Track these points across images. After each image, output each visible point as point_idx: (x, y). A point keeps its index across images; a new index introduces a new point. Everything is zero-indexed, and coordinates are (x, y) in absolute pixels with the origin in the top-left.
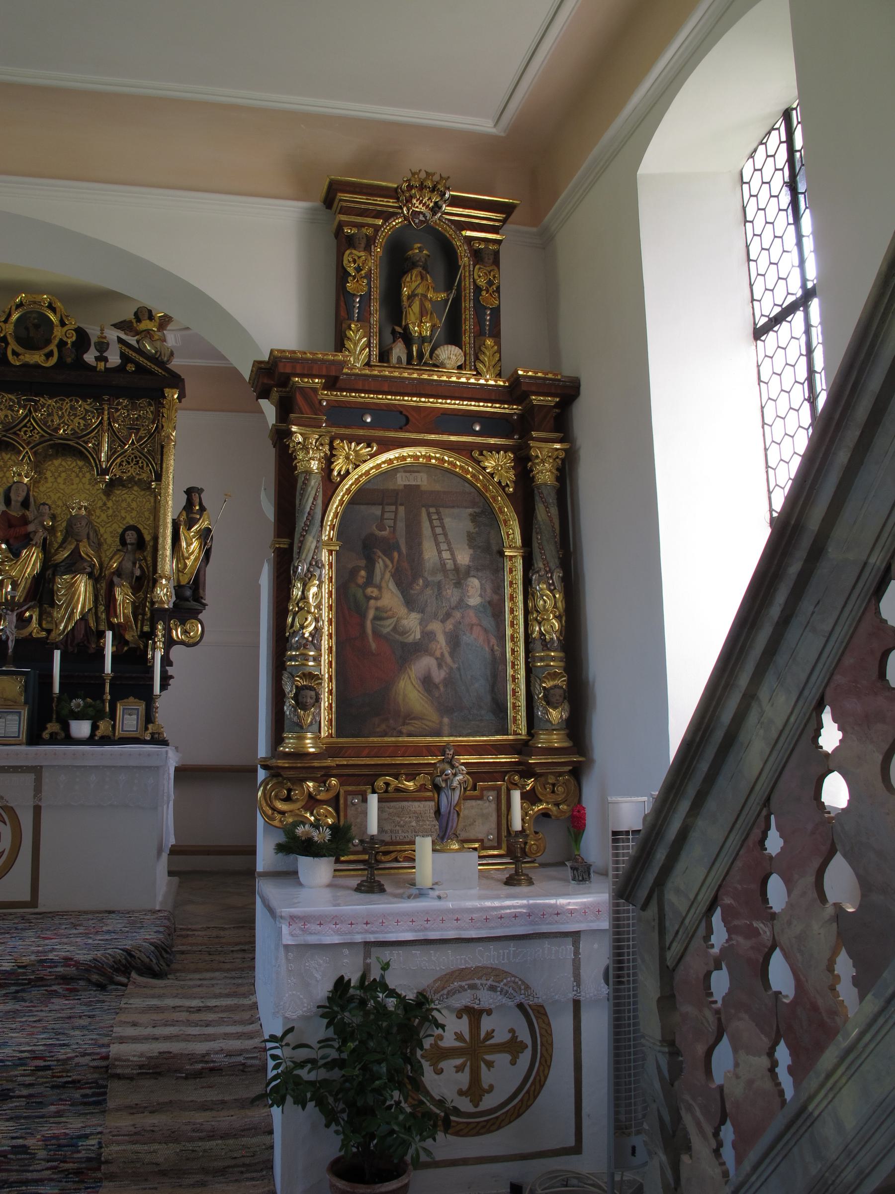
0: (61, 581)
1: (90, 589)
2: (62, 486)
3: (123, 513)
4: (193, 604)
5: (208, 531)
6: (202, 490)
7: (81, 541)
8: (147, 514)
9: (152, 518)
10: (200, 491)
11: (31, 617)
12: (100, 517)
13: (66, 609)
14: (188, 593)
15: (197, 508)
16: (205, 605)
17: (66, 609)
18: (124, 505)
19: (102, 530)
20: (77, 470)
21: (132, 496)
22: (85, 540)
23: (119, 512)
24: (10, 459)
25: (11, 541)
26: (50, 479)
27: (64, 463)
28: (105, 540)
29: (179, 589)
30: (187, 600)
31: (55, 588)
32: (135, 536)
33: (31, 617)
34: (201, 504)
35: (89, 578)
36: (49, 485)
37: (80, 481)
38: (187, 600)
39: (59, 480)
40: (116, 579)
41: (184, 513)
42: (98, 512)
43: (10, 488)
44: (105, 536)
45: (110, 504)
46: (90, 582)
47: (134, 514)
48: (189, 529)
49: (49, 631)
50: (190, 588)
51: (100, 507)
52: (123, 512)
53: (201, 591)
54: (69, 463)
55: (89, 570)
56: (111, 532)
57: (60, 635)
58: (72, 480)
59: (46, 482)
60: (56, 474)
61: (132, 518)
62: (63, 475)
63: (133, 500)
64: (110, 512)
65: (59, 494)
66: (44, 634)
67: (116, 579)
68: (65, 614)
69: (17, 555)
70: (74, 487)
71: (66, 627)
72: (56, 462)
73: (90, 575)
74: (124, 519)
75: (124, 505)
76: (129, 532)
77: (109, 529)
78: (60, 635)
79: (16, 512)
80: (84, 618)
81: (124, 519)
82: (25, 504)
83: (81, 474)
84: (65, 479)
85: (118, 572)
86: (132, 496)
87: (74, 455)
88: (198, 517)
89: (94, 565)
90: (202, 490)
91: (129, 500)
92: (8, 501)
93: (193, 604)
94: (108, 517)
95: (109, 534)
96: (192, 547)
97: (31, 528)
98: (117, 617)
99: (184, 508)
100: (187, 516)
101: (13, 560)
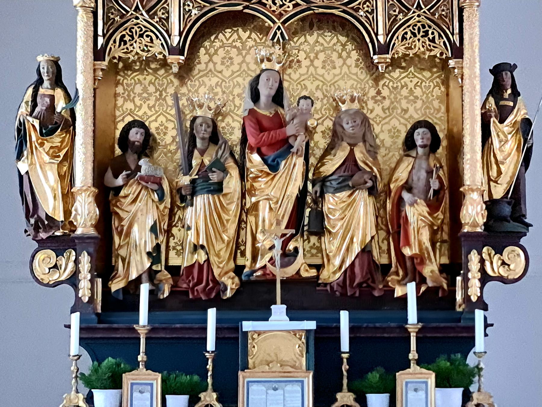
0: (333, 202)
1: (371, 210)
2: (320, 71)
3: (404, 104)
4: (513, 226)
5: (527, 124)
6: (515, 66)
7: (355, 145)
8: (436, 104)
9: (443, 109)
10: (512, 68)
11: (296, 249)
12: (374, 111)
13: (344, 238)
14: (507, 210)
15: (509, 91)
16: (528, 225)
17: (344, 238)
18: (405, 92)
19: (377, 129)
20: (339, 48)
21: (415, 80)
22: (361, 144)
23: (399, 102)
24: (249, 37)
25: (264, 149)
26: (305, 63)
27: (320, 39)
28: (382, 141)
29: (491, 205)
30: (504, 219)
31: (325, 209)
32: (429, 135)
33: (296, 249)
34: (514, 86)
35: (370, 194)
36: (303, 70)
37: (344, 63)
38: (504, 219)
39: (317, 63)
40: (406, 196)
41: (491, 100)
42: (371, 104)
43: (258, 76)
44: (382, 136)
45: (385, 92)
46: (370, 201)
47: (419, 103)
48: (502, 121)
49: (319, 267)
50: (509, 203)
51: (373, 98)
52: (404, 102)
53: (522, 206)
54: (328, 39)
55: (370, 184)
56: (390, 131)
57: (334, 273)
58: (333, 62)
59: (300, 66)
60: (312, 55)
61: (416, 110)
62: (322, 56)
63: (416, 85)
64: (387, 103)
65: (317, 83)
66: (313, 273)
67: (406, 196)
68: (341, 244)
69: (274, 168)
70: (337, 71)
71: (343, 262)
72: (311, 39)
73: (372, 191)
74: (406, 111)
75: (405, 92)
76: (420, 130)
77: (386, 127)
78: (334, 273)
79: (265, 110)
80: (366, 251)
81: (406, 111)
82: (278, 98)
83: (344, 54)
84: (324, 62)
85: (408, 187)
86: (415, 80)
87: (334, 29)
88: (511, 104)
89: (376, 176)
90: (515, 66)
91: (411, 85)
92: (255, 96)
93: (513, 226)
94: (384, 110)
95: (388, 132)
96: (506, 146)
97: (290, 130)
98: (408, 243)
99: (491, 93)
100: (497, 104)
101: (268, 174)
